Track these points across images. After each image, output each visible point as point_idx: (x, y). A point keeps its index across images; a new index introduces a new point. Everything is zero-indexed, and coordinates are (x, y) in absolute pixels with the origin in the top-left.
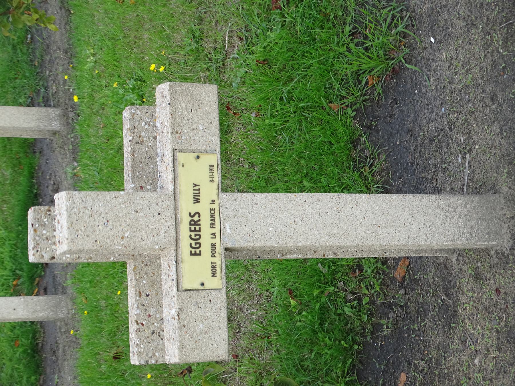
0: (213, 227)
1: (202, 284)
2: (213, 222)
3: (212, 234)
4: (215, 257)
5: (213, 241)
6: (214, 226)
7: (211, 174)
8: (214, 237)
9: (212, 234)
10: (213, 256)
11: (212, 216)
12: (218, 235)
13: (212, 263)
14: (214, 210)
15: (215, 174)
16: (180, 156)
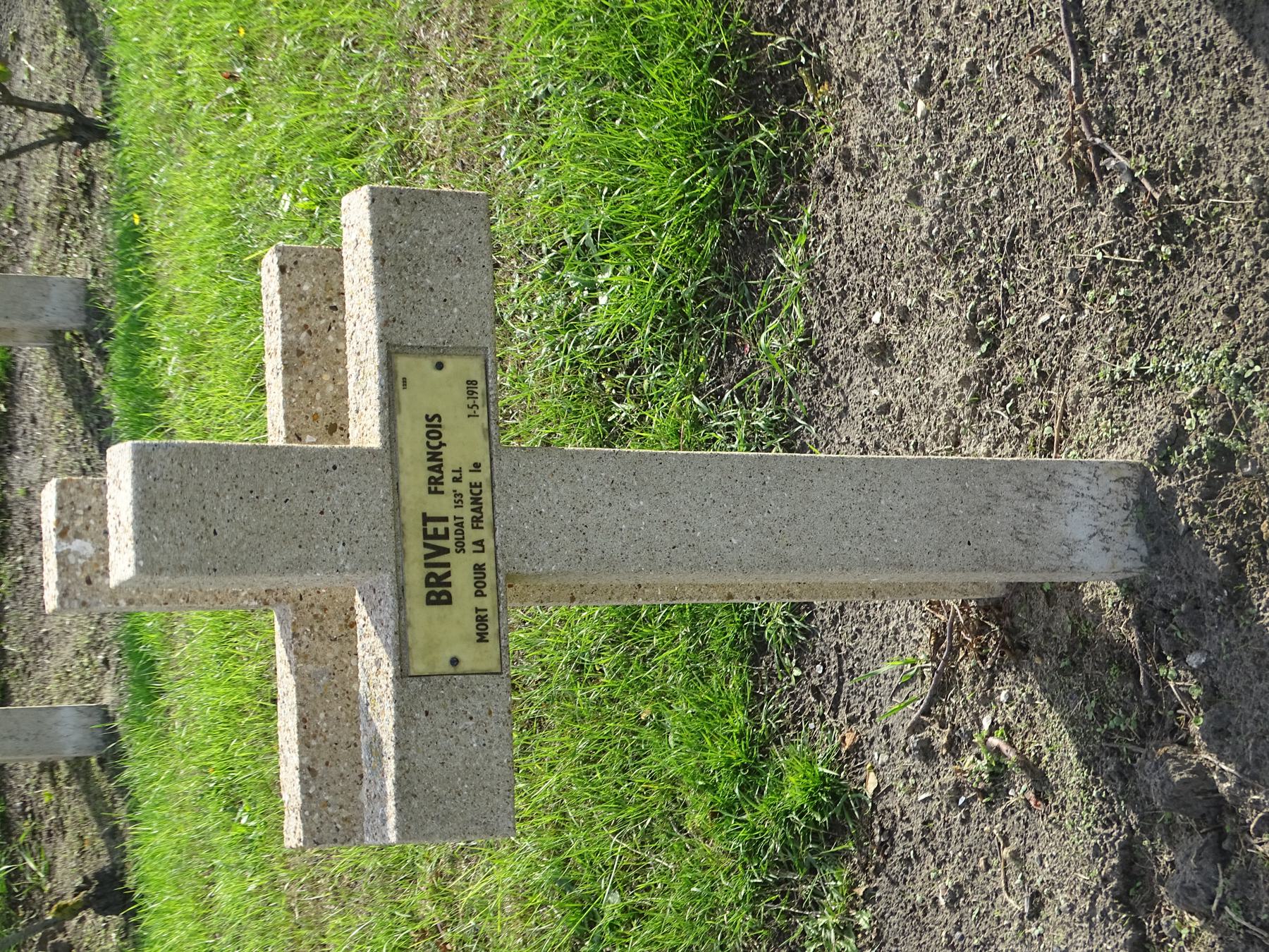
0: (478, 528)
3: (474, 543)
7: (471, 402)
8: (480, 548)
9: (474, 543)
10: (479, 593)
11: (476, 500)
12: (489, 545)
13: (477, 610)
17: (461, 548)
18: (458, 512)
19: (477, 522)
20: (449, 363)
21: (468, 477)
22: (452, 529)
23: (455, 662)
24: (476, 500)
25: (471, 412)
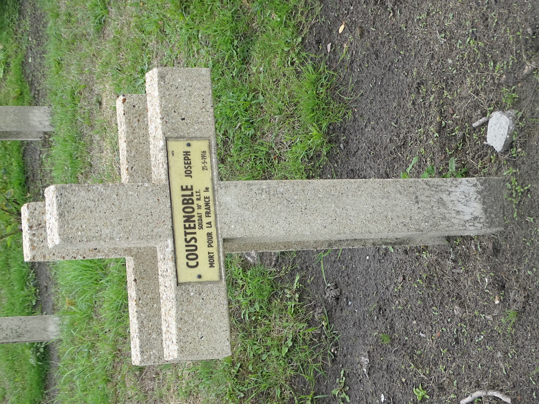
0: (208, 216)
1: (200, 277)
2: (208, 211)
3: (207, 223)
4: (212, 246)
5: (209, 230)
6: (209, 215)
8: (210, 226)
9: (207, 223)
10: (210, 246)
11: (207, 204)
12: (213, 224)
13: (209, 253)
14: (209, 198)
15: (208, 160)
16: (170, 143)
17: (201, 227)
18: (200, 211)
19: (208, 214)
20: (194, 143)
21: (203, 194)
22: (196, 218)
23: (200, 277)
24: (207, 204)
25: (203, 165)
